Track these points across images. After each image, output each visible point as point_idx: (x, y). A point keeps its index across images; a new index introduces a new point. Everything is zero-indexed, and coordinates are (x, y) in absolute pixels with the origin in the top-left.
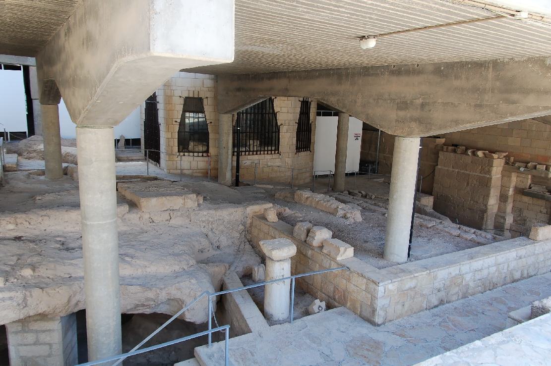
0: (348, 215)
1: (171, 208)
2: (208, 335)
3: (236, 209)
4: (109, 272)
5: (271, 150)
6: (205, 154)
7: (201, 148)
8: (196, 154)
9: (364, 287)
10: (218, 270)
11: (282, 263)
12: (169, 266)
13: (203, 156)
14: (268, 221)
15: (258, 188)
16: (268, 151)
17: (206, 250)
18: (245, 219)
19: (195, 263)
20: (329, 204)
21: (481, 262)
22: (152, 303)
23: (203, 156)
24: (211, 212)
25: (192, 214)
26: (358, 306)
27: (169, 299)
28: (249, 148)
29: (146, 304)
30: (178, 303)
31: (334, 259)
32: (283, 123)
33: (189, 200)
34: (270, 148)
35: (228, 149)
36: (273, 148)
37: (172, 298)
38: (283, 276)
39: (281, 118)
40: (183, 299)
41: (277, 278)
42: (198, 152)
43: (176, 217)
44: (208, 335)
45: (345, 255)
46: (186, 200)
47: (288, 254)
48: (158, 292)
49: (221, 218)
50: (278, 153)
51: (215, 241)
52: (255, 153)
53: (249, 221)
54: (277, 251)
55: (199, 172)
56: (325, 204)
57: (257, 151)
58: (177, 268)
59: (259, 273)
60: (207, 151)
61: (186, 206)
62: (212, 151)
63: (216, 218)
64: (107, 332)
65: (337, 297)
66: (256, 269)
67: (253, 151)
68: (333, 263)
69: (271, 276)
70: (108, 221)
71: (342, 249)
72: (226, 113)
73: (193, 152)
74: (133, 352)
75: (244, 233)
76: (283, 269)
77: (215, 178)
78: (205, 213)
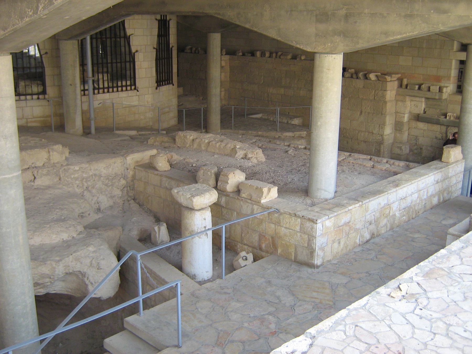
0: (250, 156)
1: (33, 165)
2: (138, 302)
3: (113, 160)
4: (21, 237)
5: (126, 86)
6: (41, 96)
7: (35, 89)
8: (29, 97)
9: (298, 228)
10: (114, 234)
11: (204, 211)
12: (56, 234)
13: (38, 98)
14: (157, 170)
15: (119, 136)
16: (122, 86)
17: (87, 214)
18: (126, 171)
19: (83, 229)
20: (223, 145)
21: (405, 189)
22: (48, 280)
23: (38, 98)
24: (84, 165)
25: (61, 170)
26: (292, 250)
27: (67, 273)
28: (98, 85)
29: (40, 282)
30: (77, 276)
31: (258, 203)
32: (139, 49)
33: (55, 153)
34: (124, 83)
35: (76, 87)
36: (129, 83)
37: (71, 271)
38: (205, 227)
39: (135, 44)
40: (85, 270)
41: (199, 231)
42: (32, 94)
43: (41, 177)
44: (138, 302)
45: (269, 196)
46: (51, 153)
47: (209, 201)
48: (54, 266)
49: (97, 172)
50: (135, 89)
51: (93, 202)
52: (106, 90)
53: (130, 173)
54: (198, 197)
55: (35, 122)
56: (218, 144)
57: (108, 88)
58: (65, 236)
59: (161, 233)
60: (44, 92)
61: (52, 162)
62: (51, 91)
63: (91, 173)
64: (25, 311)
65: (263, 246)
66: (156, 228)
67: (104, 88)
68: (255, 207)
69: (190, 229)
70: (15, 174)
71: (265, 190)
72: (71, 38)
73: (26, 95)
74: (60, 329)
75: (125, 189)
76: (205, 219)
77: (61, 128)
78: (77, 168)
